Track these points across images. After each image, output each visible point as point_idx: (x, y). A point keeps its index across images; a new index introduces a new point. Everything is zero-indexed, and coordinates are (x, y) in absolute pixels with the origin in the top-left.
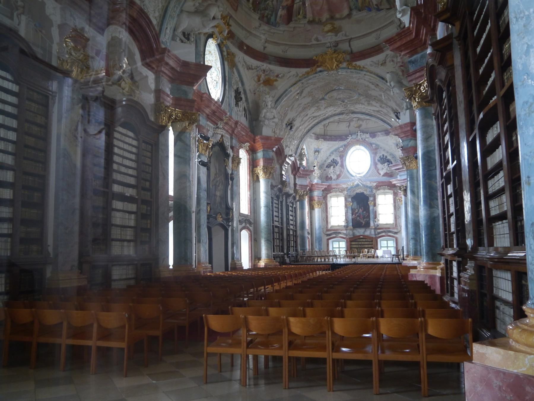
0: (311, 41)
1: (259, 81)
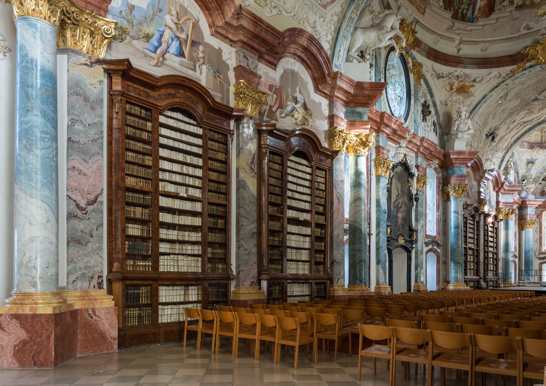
1: (452, 89)
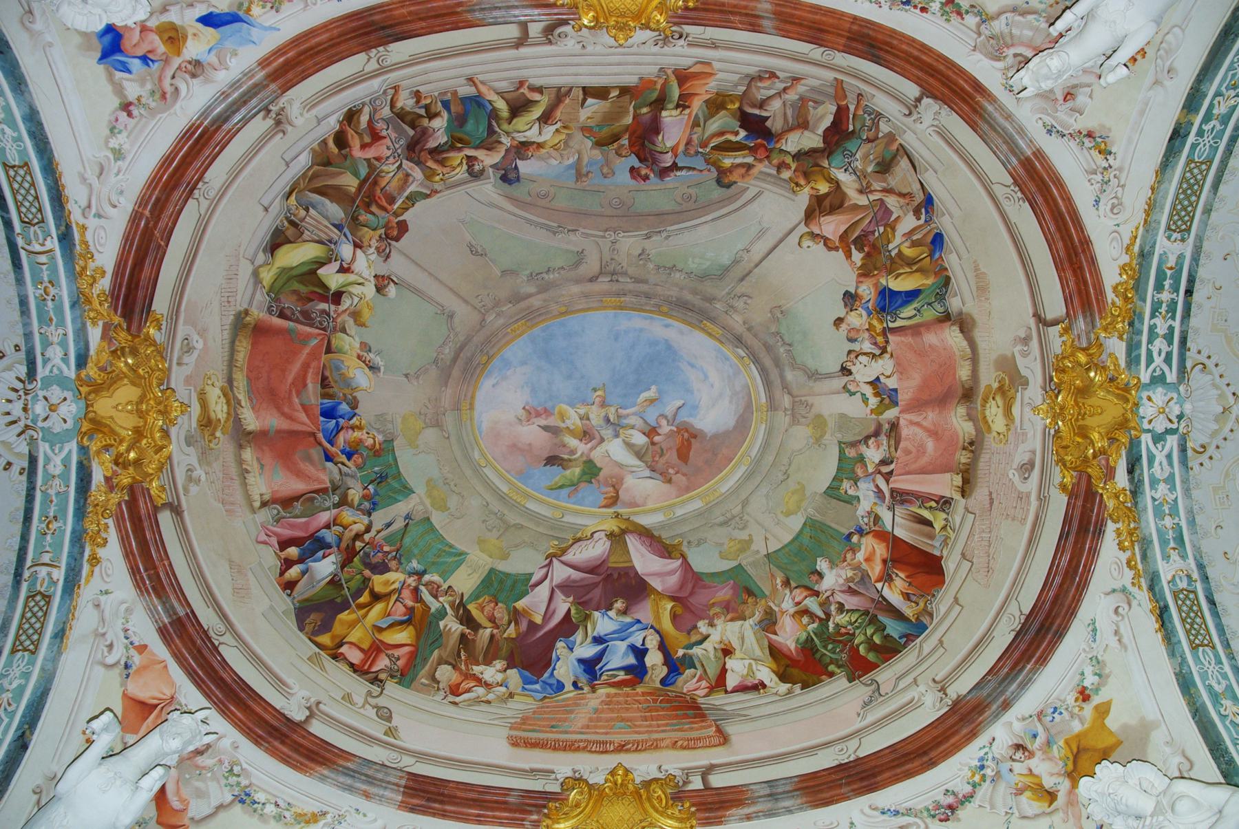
0: (1028, 495)
